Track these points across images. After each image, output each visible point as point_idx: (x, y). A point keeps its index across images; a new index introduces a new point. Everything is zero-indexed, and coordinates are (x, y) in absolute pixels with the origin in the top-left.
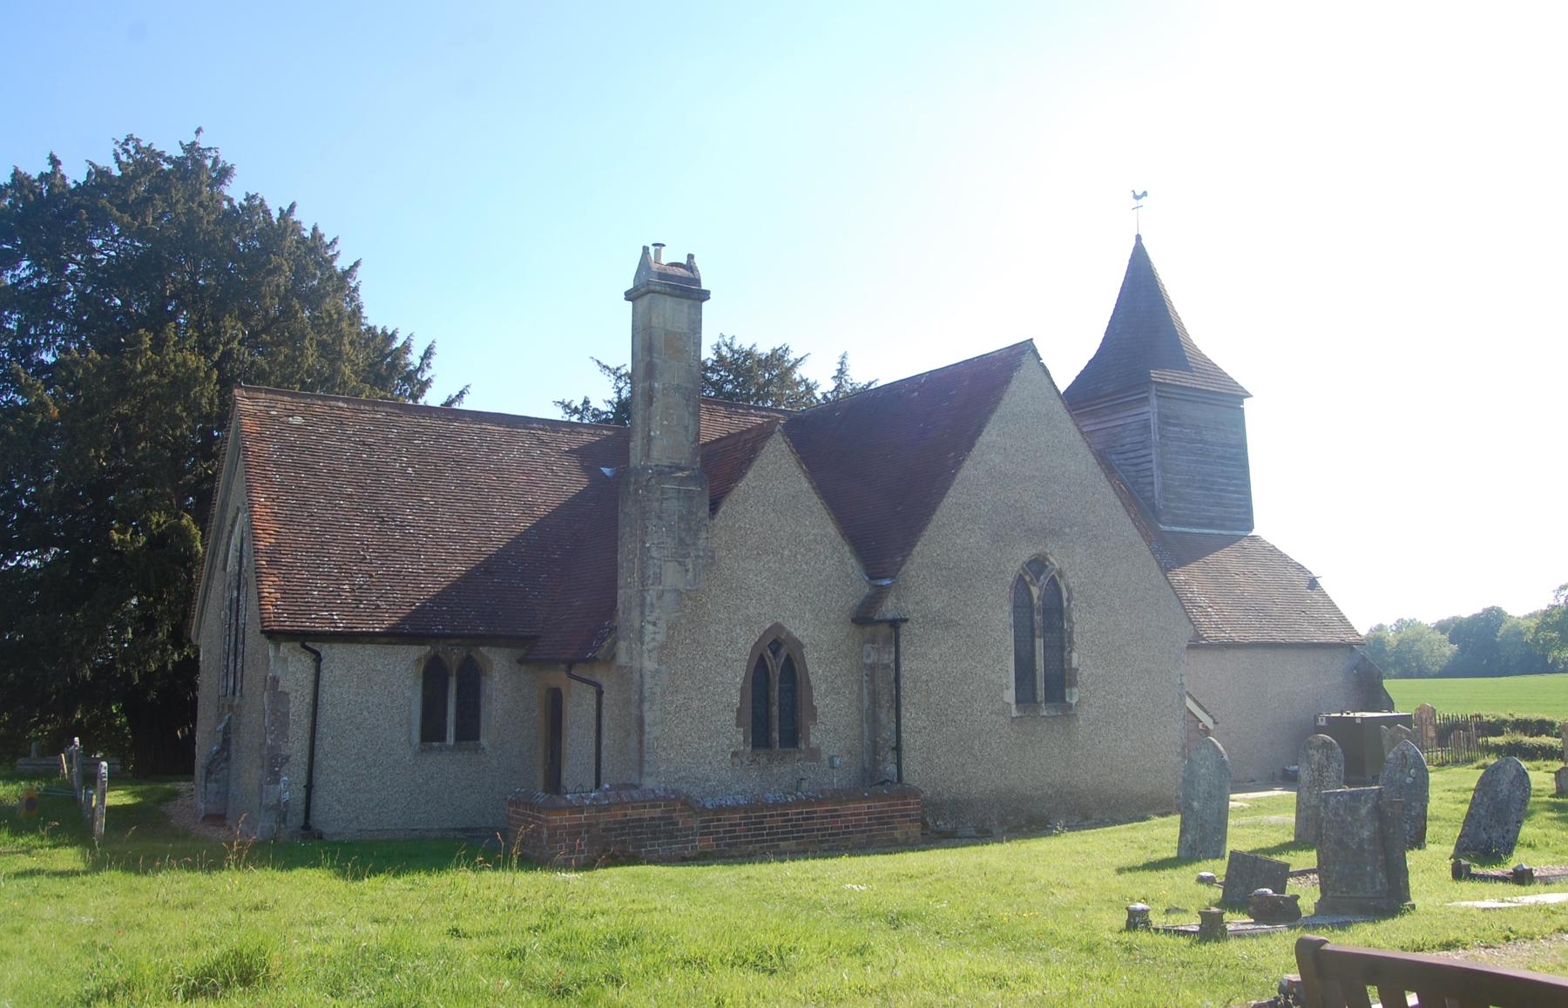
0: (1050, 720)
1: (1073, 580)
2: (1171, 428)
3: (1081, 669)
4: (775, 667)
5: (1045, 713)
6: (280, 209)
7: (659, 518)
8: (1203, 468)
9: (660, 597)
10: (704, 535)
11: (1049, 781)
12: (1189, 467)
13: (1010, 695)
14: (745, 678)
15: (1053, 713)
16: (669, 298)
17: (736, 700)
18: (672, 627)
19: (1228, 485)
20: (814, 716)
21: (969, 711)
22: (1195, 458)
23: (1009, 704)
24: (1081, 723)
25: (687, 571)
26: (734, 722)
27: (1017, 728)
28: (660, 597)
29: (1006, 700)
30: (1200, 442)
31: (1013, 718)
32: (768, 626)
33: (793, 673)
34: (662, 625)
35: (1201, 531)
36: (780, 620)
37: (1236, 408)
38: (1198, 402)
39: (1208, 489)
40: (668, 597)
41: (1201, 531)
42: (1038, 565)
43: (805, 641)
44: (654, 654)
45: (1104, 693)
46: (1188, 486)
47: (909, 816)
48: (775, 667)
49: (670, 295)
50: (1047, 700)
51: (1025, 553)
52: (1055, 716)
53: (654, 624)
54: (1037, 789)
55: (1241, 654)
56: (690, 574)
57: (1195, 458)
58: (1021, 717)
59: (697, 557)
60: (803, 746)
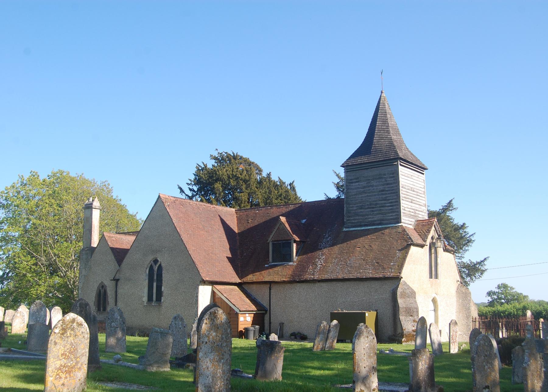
0: (154, 306)
1: (163, 265)
2: (354, 184)
3: (164, 291)
4: (102, 291)
5: (154, 304)
6: (193, 174)
7: (82, 259)
8: (370, 198)
9: (82, 277)
10: (89, 262)
11: (153, 324)
12: (362, 199)
13: (145, 299)
14: (96, 295)
15: (156, 304)
16: (87, 210)
17: (94, 300)
18: (83, 283)
19: (385, 203)
20: (108, 304)
21: (134, 303)
22: (366, 195)
23: (143, 301)
24: (163, 307)
25: (86, 271)
26: (93, 305)
27: (145, 308)
28: (82, 277)
29: (143, 300)
30: (369, 187)
31: (144, 306)
32: (100, 282)
33: (105, 292)
34: (82, 283)
35: (367, 228)
36: (102, 281)
37: (392, 165)
38: (369, 168)
39: (373, 208)
40: (83, 277)
41: (367, 228)
42: (156, 261)
43: (107, 285)
44: (81, 290)
45: (170, 299)
46: (361, 208)
47: (102, 328)
48: (102, 291)
49: (87, 209)
50: (156, 301)
51: (151, 258)
52: (156, 306)
53: (81, 283)
54: (150, 326)
55: (324, 285)
56: (87, 272)
57: (366, 195)
58: (147, 305)
59: (88, 267)
60: (106, 311)
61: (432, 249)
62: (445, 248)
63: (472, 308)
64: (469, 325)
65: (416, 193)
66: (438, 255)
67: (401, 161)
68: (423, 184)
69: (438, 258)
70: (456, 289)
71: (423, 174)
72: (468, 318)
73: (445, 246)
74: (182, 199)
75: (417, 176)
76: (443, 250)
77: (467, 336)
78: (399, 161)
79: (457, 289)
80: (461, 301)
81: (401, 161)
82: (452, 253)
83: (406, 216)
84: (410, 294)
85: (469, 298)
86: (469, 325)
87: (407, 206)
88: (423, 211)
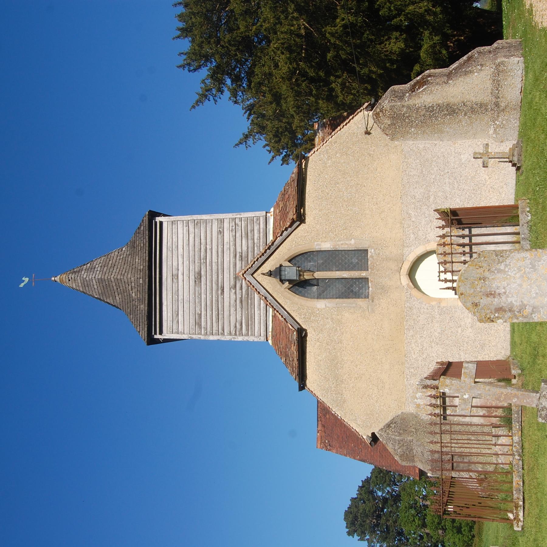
61: (303, 279)
62: (296, 221)
63: (429, 101)
64: (472, 108)
65: (202, 261)
66: (315, 250)
67: (153, 334)
68: (180, 225)
69: (322, 250)
70: (385, 136)
71: (161, 223)
72: (454, 111)
73: (293, 222)
74: (318, 406)
75: (170, 254)
76: (303, 225)
77: (498, 116)
78: (156, 337)
79: (387, 135)
80: (413, 130)
81: (153, 334)
82: (306, 165)
83: (251, 317)
84: (405, 448)
85: (405, 109)
86: (472, 108)
87: (232, 310)
88: (234, 234)
